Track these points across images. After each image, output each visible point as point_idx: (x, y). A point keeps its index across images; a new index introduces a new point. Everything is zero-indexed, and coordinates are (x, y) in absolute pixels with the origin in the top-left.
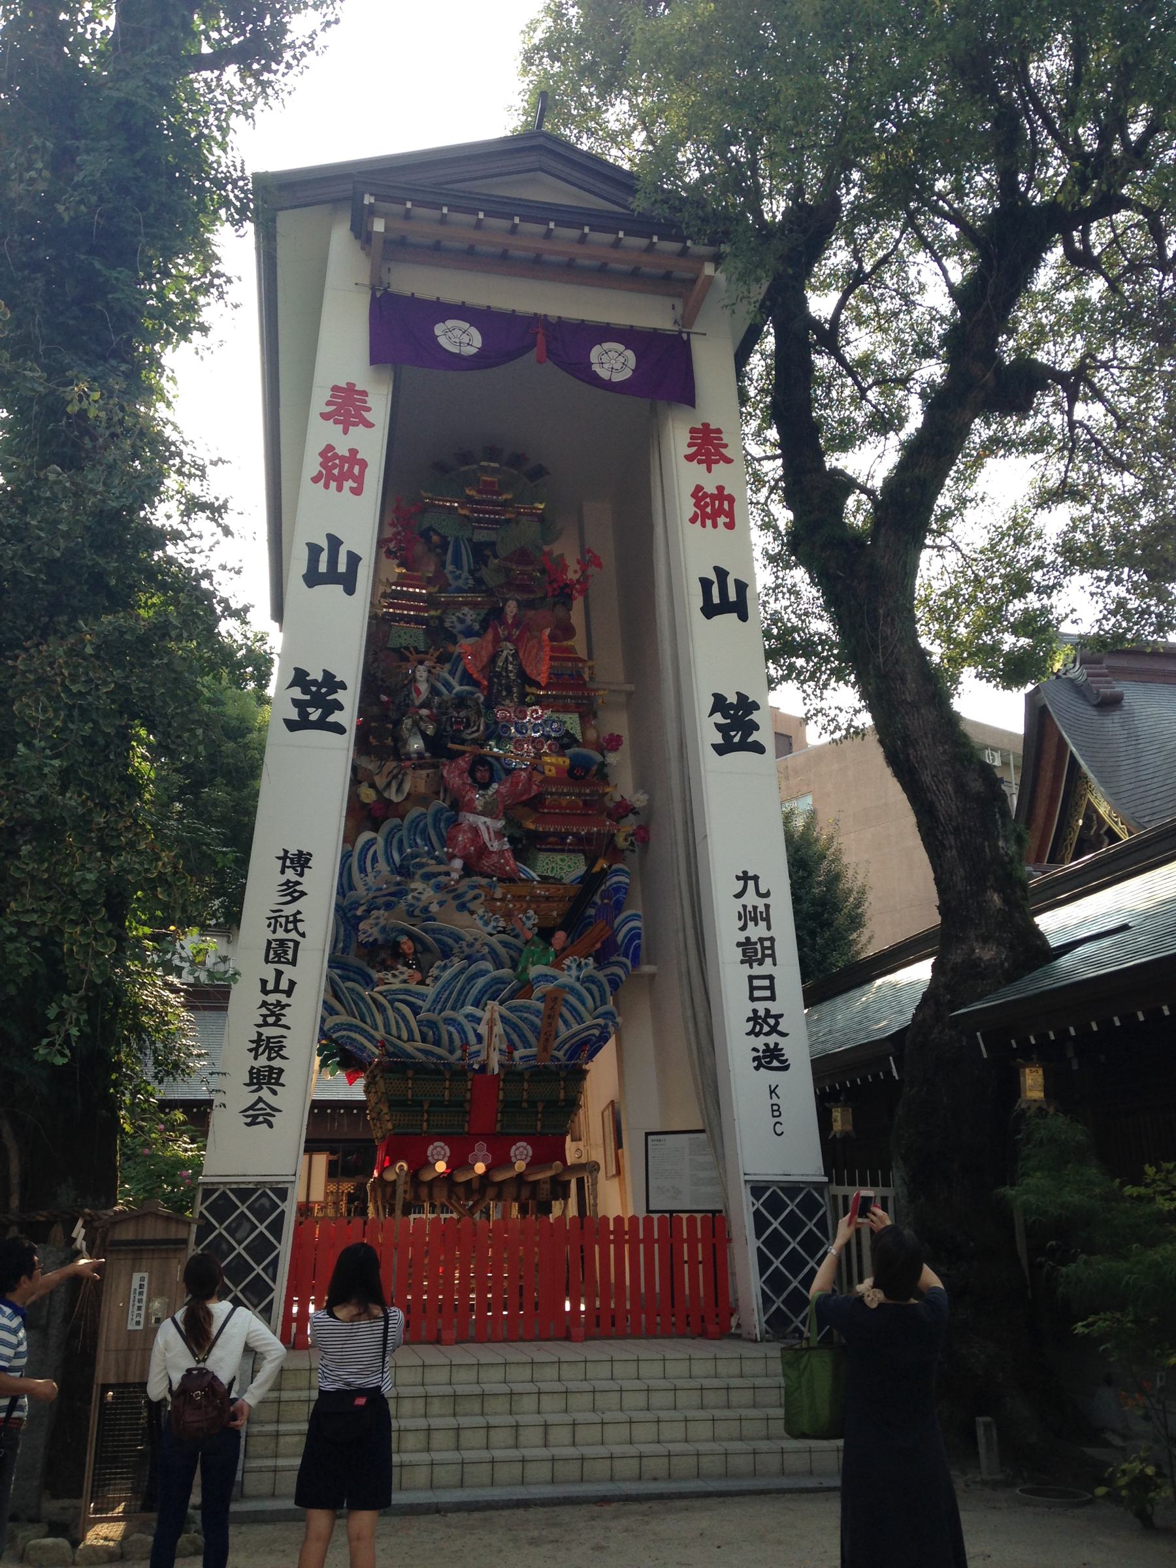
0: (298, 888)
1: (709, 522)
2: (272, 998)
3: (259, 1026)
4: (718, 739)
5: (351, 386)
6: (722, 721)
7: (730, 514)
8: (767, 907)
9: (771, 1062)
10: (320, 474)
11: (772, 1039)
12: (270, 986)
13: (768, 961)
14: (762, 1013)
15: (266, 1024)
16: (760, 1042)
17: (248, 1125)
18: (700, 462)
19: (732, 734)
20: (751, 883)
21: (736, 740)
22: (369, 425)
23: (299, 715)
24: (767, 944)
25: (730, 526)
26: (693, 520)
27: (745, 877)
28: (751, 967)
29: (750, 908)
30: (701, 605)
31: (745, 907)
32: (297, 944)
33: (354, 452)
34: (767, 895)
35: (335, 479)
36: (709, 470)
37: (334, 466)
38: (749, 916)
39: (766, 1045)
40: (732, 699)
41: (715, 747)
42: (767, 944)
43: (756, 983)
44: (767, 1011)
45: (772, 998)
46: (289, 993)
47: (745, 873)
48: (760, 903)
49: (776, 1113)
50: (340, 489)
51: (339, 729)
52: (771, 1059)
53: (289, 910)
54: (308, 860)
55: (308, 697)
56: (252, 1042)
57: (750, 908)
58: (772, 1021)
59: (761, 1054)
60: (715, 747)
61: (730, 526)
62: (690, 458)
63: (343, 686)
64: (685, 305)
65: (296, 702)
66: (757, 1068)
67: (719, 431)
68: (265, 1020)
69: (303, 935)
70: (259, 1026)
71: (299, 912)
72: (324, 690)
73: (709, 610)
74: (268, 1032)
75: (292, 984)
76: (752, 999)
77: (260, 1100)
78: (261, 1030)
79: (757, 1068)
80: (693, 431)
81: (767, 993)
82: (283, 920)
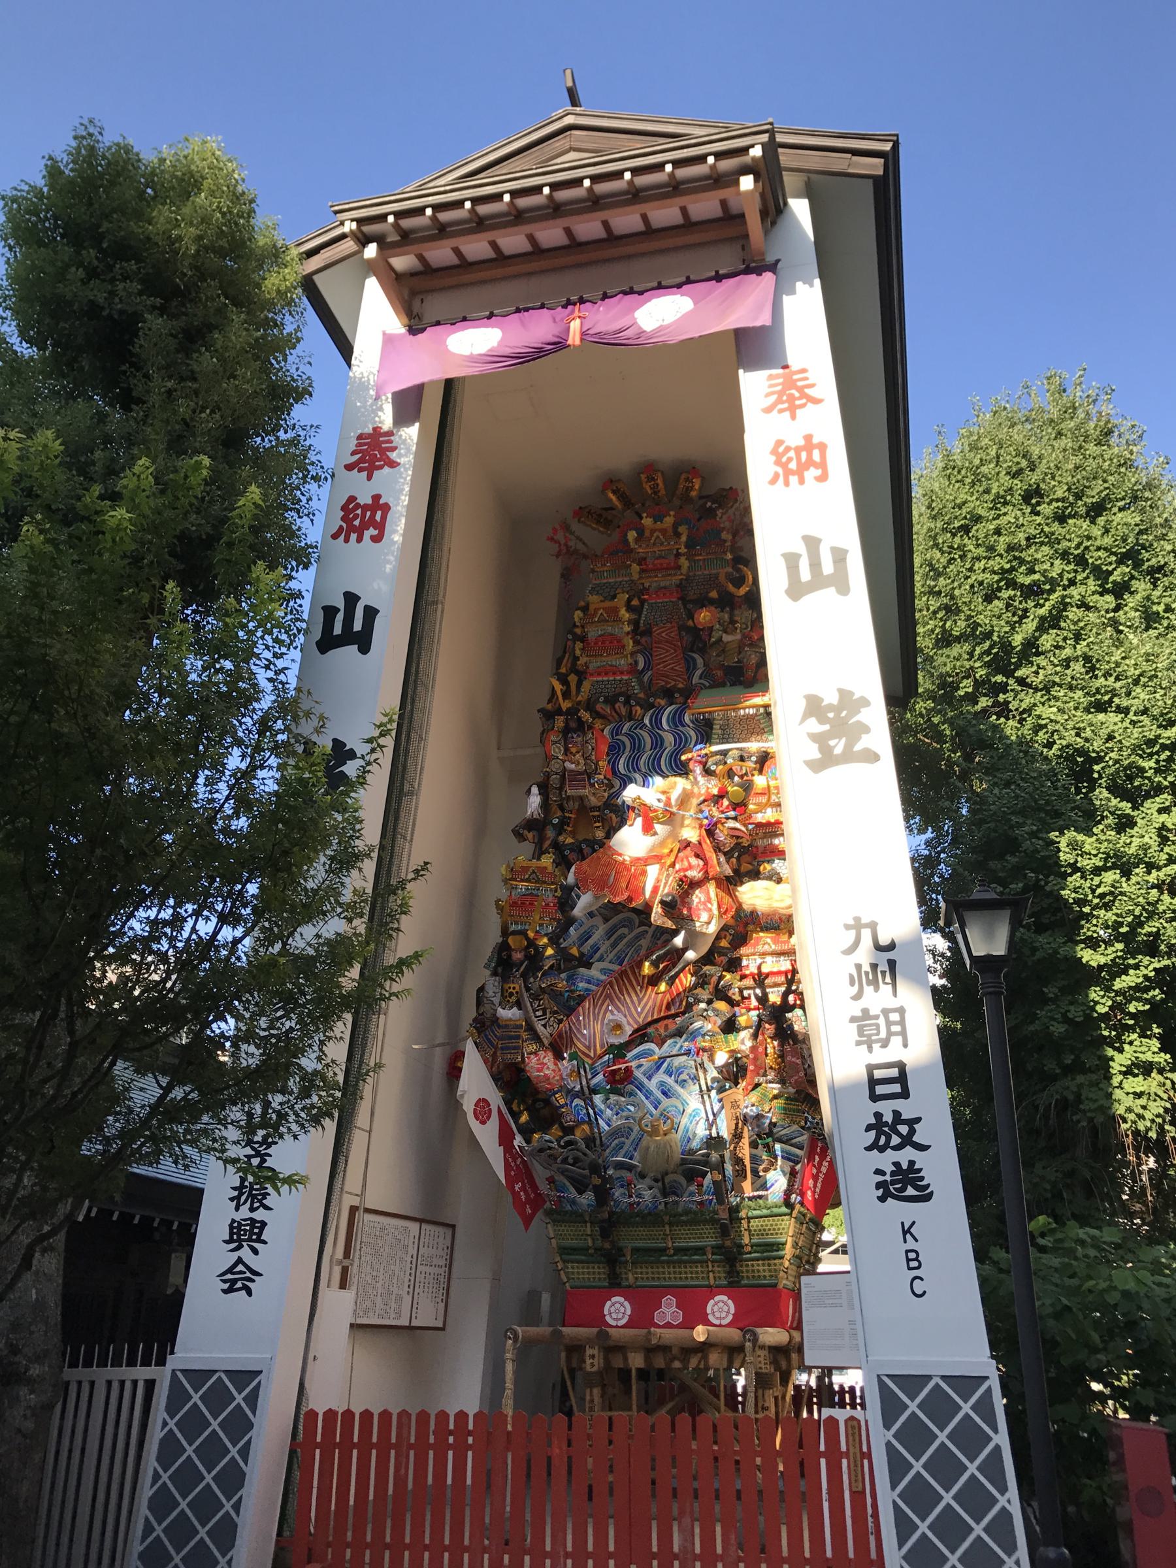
1: (794, 479)
9: (903, 1189)
11: (906, 1155)
13: (896, 1041)
14: (888, 1118)
16: (886, 1160)
17: (225, 1292)
18: (781, 411)
24: (895, 1017)
27: (857, 925)
28: (870, 1049)
31: (858, 967)
33: (376, 498)
36: (793, 417)
37: (356, 517)
39: (897, 1164)
42: (895, 1017)
44: (897, 1114)
45: (905, 1094)
49: (914, 1264)
52: (904, 1184)
56: (234, 1189)
58: (904, 1129)
59: (888, 1178)
66: (882, 1199)
76: (874, 1098)
77: (240, 1261)
79: (882, 1199)
81: (896, 1088)
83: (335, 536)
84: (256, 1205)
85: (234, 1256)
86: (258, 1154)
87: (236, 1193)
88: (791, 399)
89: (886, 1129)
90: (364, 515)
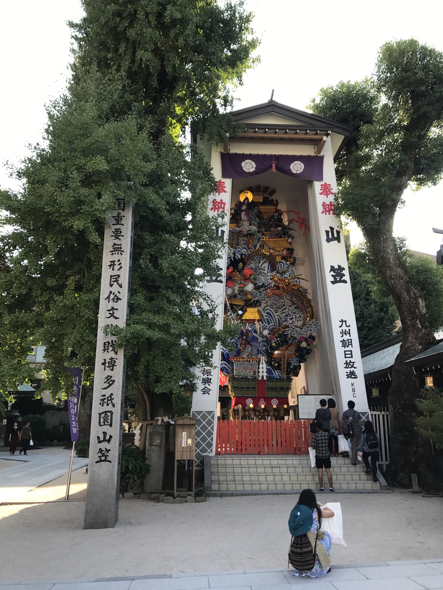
1: (327, 213)
8: (349, 330)
11: (352, 369)
13: (350, 346)
14: (348, 362)
16: (348, 370)
18: (324, 195)
20: (344, 323)
21: (338, 279)
24: (350, 341)
26: (323, 213)
27: (342, 321)
29: (344, 330)
31: (342, 330)
34: (349, 326)
36: (327, 197)
38: (344, 333)
39: (350, 371)
40: (336, 267)
41: (331, 282)
42: (350, 341)
43: (346, 353)
44: (350, 361)
45: (352, 357)
47: (342, 320)
48: (347, 329)
52: (352, 375)
58: (352, 364)
60: (331, 282)
62: (321, 194)
64: (318, 148)
66: (348, 378)
67: (330, 185)
73: (328, 240)
76: (346, 357)
77: (206, 387)
81: (350, 356)
85: (204, 386)
88: (327, 192)
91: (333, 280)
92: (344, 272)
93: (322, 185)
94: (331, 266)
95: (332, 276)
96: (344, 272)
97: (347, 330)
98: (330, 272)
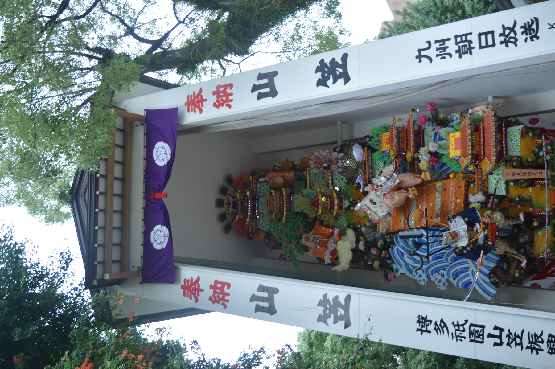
0: (438, 323)
1: (230, 98)
2: (505, 340)
3: (522, 348)
4: (341, 81)
5: (182, 287)
6: (331, 80)
7: (226, 86)
8: (436, 42)
9: (533, 30)
10: (223, 304)
12: (498, 341)
13: (469, 37)
14: (502, 38)
15: (521, 344)
16: (521, 38)
18: (202, 106)
19: (338, 73)
20: (423, 53)
22: (198, 279)
23: (342, 320)
24: (459, 39)
25: (231, 86)
27: (419, 57)
28: (474, 48)
29: (438, 52)
30: (271, 98)
31: (437, 56)
32: (472, 325)
34: (429, 42)
35: (224, 297)
36: (206, 100)
37: (218, 296)
38: (443, 53)
39: (523, 33)
40: (319, 75)
41: (346, 82)
42: (459, 39)
43: (483, 44)
44: (501, 35)
45: (492, 32)
46: (502, 330)
47: (417, 57)
48: (434, 46)
50: (228, 294)
51: (348, 298)
52: (531, 30)
53: (452, 329)
54: (422, 318)
55: (332, 315)
56: (532, 352)
57: (438, 52)
58: (507, 32)
59: (528, 36)
60: (346, 82)
61: (231, 86)
62: (201, 111)
63: (325, 296)
65: (335, 322)
66: (538, 38)
67: (188, 97)
68: (519, 344)
69: (466, 321)
70: (522, 348)
71: (453, 323)
72: (328, 306)
73: (273, 93)
74: (526, 343)
75: (496, 328)
76: (494, 45)
78: (525, 346)
79: (538, 38)
80: (188, 111)
81: (490, 36)
82: (458, 333)
83: (225, 307)
84: (540, 340)
86: (514, 340)
87: (534, 351)
88: (198, 102)
89: (507, 39)
90: (218, 293)
91: (342, 80)
92: (327, 61)
93: (188, 111)
94: (318, 86)
95: (334, 82)
96: (327, 61)
97: (438, 45)
98: (328, 86)
